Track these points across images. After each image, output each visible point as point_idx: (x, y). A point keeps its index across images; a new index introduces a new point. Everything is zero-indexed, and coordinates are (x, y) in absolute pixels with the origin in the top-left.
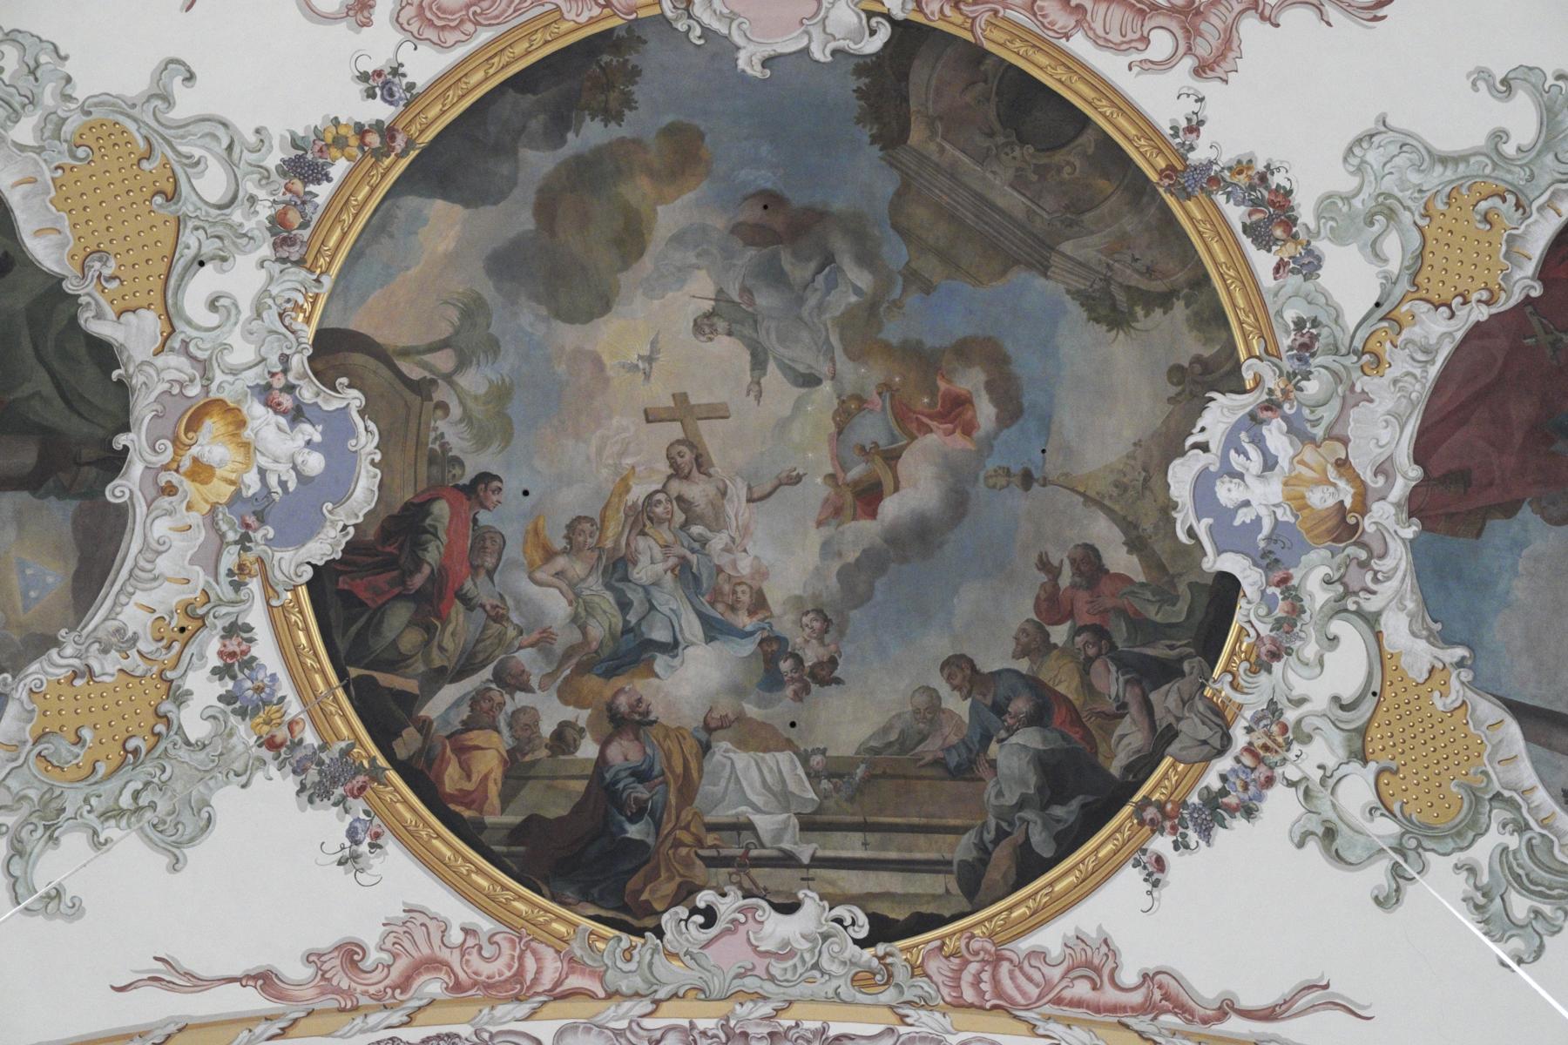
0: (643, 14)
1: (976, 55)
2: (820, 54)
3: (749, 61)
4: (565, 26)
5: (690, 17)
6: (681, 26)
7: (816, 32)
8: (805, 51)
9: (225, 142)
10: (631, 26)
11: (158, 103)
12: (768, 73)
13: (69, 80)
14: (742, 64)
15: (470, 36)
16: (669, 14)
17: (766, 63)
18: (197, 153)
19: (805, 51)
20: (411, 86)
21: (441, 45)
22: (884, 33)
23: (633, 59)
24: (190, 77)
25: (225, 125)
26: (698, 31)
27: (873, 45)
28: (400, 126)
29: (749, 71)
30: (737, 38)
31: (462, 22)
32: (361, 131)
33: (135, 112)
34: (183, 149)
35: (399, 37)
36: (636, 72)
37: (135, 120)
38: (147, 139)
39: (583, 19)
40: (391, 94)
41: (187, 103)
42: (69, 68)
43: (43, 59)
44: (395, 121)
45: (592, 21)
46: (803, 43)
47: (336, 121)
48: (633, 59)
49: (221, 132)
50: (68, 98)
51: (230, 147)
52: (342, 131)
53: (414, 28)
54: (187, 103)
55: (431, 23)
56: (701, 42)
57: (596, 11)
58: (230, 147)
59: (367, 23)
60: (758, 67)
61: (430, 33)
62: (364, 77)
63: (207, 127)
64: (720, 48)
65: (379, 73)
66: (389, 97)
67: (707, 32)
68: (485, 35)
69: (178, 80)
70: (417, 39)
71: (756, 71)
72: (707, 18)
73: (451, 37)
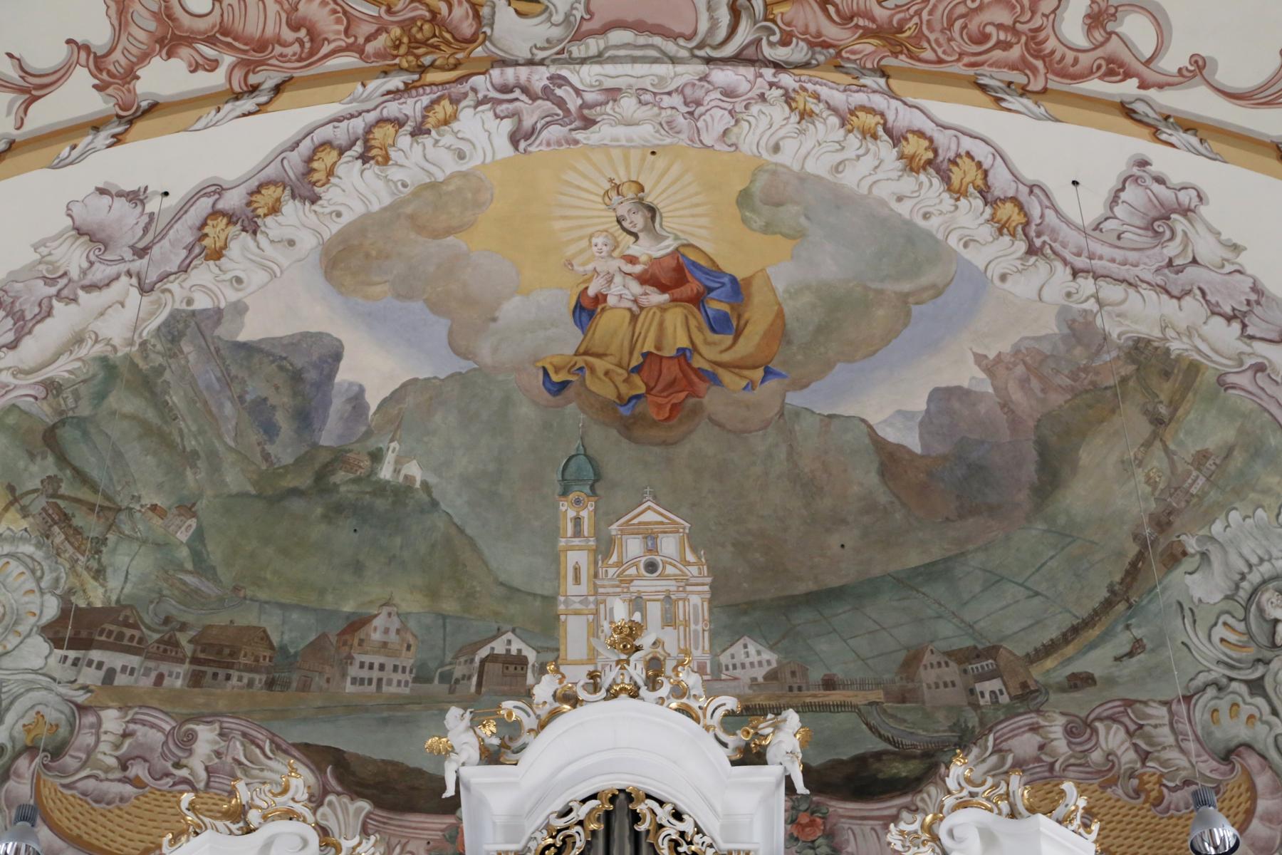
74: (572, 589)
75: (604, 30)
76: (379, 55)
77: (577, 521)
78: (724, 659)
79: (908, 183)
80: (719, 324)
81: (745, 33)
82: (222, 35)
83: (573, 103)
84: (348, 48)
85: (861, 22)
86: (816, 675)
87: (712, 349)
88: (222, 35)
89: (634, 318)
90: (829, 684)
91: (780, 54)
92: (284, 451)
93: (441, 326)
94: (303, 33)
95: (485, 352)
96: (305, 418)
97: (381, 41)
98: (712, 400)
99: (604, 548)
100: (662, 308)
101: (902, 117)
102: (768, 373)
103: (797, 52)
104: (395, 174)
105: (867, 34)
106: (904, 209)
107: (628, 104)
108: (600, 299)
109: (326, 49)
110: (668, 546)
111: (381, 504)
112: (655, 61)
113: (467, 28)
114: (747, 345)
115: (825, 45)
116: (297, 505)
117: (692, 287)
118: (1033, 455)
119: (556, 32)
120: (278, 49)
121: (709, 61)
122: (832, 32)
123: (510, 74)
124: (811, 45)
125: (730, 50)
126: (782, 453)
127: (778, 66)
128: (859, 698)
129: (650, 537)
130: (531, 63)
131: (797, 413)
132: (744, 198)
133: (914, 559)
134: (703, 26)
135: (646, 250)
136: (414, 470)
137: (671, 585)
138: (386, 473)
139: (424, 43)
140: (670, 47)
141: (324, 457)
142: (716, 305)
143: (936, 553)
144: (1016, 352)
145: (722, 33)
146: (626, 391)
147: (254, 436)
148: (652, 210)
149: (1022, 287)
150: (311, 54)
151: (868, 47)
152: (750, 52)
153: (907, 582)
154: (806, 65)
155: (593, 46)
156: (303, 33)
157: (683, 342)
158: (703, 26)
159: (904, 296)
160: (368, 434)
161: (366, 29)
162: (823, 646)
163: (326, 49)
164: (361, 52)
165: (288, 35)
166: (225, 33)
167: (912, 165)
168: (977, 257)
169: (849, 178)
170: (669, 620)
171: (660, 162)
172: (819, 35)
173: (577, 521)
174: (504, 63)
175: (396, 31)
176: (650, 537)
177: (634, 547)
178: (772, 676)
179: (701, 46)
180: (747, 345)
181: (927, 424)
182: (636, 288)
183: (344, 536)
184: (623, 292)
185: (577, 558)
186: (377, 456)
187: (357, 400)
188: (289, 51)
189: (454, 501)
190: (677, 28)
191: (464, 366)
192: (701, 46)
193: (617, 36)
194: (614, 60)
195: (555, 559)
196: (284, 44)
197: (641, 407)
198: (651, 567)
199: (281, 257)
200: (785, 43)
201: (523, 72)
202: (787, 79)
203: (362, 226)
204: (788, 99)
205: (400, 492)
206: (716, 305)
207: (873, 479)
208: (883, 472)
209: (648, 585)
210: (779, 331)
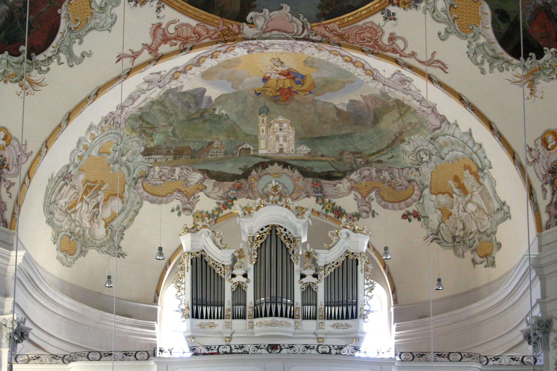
0: (316, 24)
1: (222, 15)
2: (266, 11)
3: (287, 9)
4: (338, 23)
5: (303, 22)
6: (305, 19)
7: (268, 17)
8: (270, 11)
9: (435, 13)
10: (320, 21)
11: (449, 31)
12: (281, 5)
13: (468, 47)
14: (289, 8)
15: (364, 24)
16: (309, 23)
17: (282, 8)
18: (443, 14)
19: (270, 11)
20: (382, 14)
21: (372, 23)
22: (248, 18)
23: (320, 11)
24: (439, 34)
25: (433, 18)
26: (301, 18)
27: (251, 14)
28: (387, 3)
29: (286, 5)
30: (290, 15)
31: (366, 28)
32: (398, 5)
33: (455, 31)
34: (445, 16)
35: (383, 28)
36: (320, 7)
37: (456, 29)
38: (454, 23)
39: (333, 24)
40: (388, 13)
41: (442, 27)
42: (467, 50)
43: (472, 55)
44: (388, 5)
45: (330, 23)
46: (271, 14)
47: (404, 9)
48: (320, 11)
49: (435, 16)
50: (470, 42)
51: (434, 12)
52: (403, 6)
53: (379, 30)
54: (442, 27)
55: (374, 30)
56: (300, 15)
57: (329, 26)
58: (434, 12)
59: (391, 34)
60: (284, 6)
61: (375, 27)
62: (395, 19)
63: (439, 19)
64: (295, 12)
65: (391, 19)
66: (389, 12)
67: (298, 17)
68: (360, 23)
69: (442, 34)
70: (378, 26)
71: (285, 6)
72: (298, 21)
73: (369, 25)
74: (261, 134)
75: (271, 31)
76: (215, 38)
77: (263, 120)
78: (298, 149)
79: (345, 64)
80: (298, 83)
81: (306, 33)
82: (177, 37)
83: (263, 46)
84: (208, 37)
85: (334, 32)
86: (320, 154)
87: (296, 87)
88: (177, 37)
89: (277, 81)
90: (322, 156)
91: (314, 38)
92: (192, 111)
93: (230, 84)
94: (197, 35)
95: (241, 88)
96: (197, 104)
97: (216, 35)
98: (296, 97)
99: (269, 126)
100: (285, 79)
101: (344, 53)
102: (310, 93)
103: (319, 38)
104: (219, 59)
105: (336, 35)
106: (344, 67)
107: (276, 46)
108: (269, 77)
109: (202, 38)
110: (285, 125)
111: (215, 119)
112: (283, 39)
113: (237, 31)
114: (304, 87)
115: (326, 37)
116: (196, 121)
117: (292, 76)
118: (373, 115)
119: (259, 31)
120: (191, 39)
121: (297, 39)
122: (327, 34)
123: (247, 42)
124: (322, 36)
125: (302, 36)
126: (313, 108)
127: (313, 41)
128: (330, 159)
129: (281, 124)
130: (253, 39)
131: (317, 101)
132: (305, 62)
133: (344, 132)
134: (295, 31)
135: (280, 69)
136: (224, 112)
137: (286, 133)
138: (217, 112)
139: (226, 35)
140: (287, 35)
141: (201, 111)
142: (297, 79)
143: (349, 131)
144: (370, 96)
145: (300, 32)
146: (275, 94)
147: (185, 109)
148: (282, 63)
149: (373, 84)
150: (199, 39)
151: (336, 38)
152: (307, 37)
153: (341, 137)
154: (320, 42)
155: (268, 34)
156: (197, 35)
157: (289, 86)
158: (295, 31)
159: (344, 82)
160: (213, 105)
161: (212, 33)
162: (322, 148)
163: (202, 38)
164: (211, 38)
165: (193, 35)
166: (178, 37)
167: (346, 61)
168: (362, 78)
169: (331, 61)
170: (285, 140)
171: (284, 55)
172: (324, 34)
173: (263, 120)
174: (246, 39)
175: (219, 33)
176: (281, 124)
177: (277, 125)
178: (309, 153)
179: (295, 35)
180: (304, 87)
181: (348, 106)
182: (278, 76)
183: (207, 126)
184: (274, 76)
185: (263, 127)
186: (215, 110)
187: (210, 99)
188: (193, 39)
189: (233, 117)
190: (289, 31)
191: (235, 91)
192: (295, 35)
193: (274, 32)
194: (273, 38)
195: (258, 128)
196: (192, 38)
197: (279, 98)
198: (281, 130)
199: (192, 76)
200: (316, 35)
201: (251, 42)
202: (316, 44)
203: (210, 69)
204: (316, 47)
205: (220, 116)
206: (297, 79)
207: (335, 115)
208: (337, 114)
209: (280, 133)
210: (313, 85)
